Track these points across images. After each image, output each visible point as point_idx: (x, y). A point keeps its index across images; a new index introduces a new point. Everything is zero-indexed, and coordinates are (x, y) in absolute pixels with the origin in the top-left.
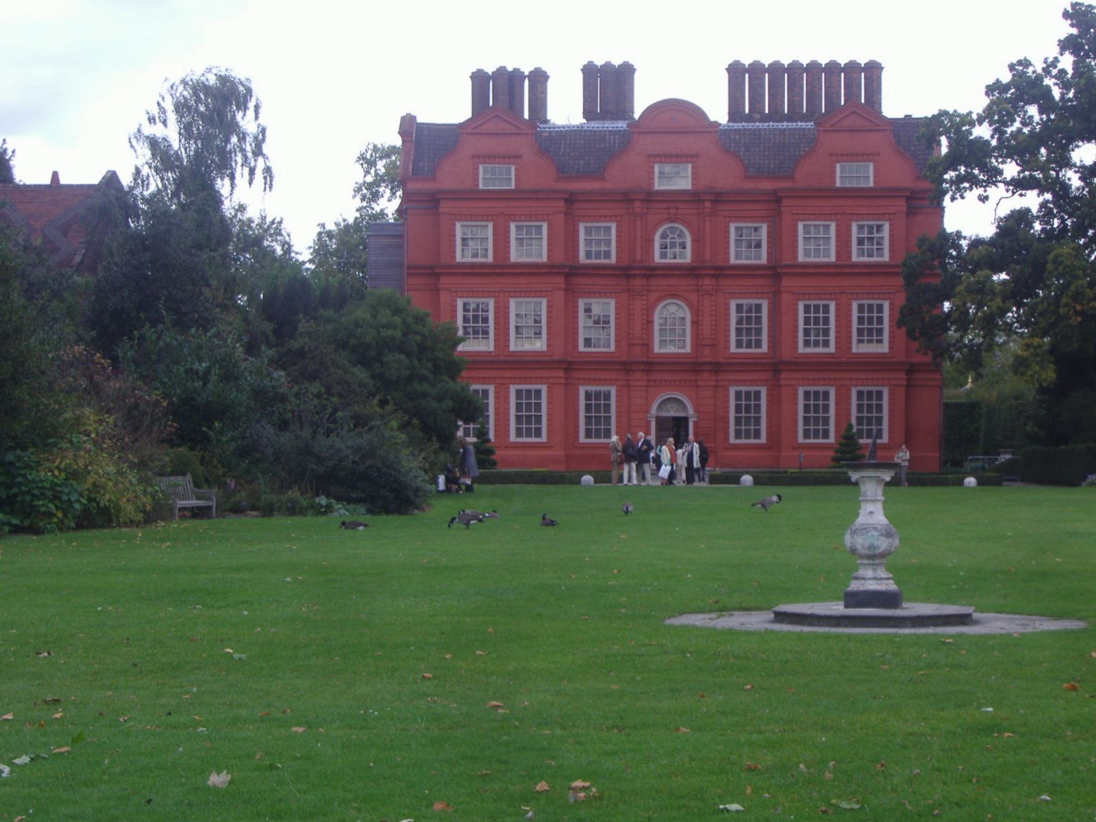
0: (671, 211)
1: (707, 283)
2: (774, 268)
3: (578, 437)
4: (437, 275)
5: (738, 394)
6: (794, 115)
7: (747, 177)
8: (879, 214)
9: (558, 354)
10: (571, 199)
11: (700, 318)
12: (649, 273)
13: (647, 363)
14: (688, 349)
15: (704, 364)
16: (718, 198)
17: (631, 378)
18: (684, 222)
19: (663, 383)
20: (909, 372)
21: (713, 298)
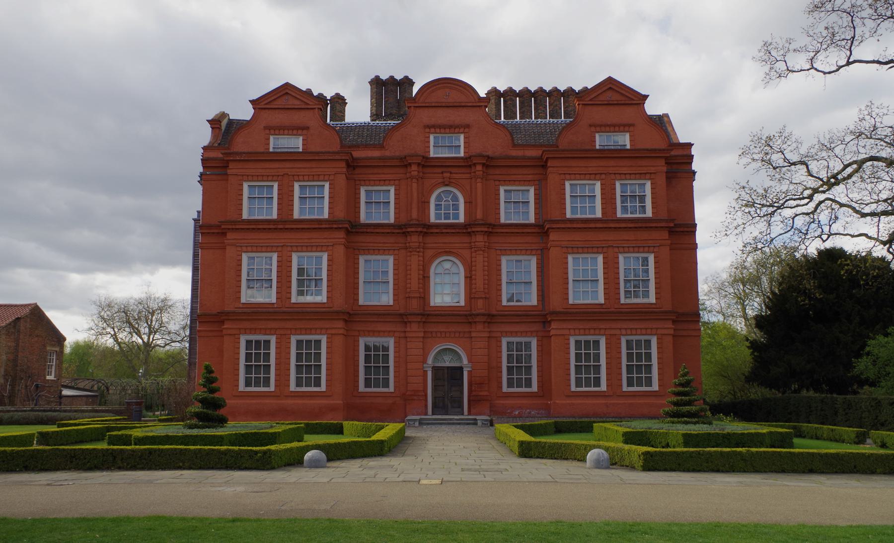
2: (541, 227)
3: (358, 386)
4: (224, 234)
7: (515, 146)
8: (641, 174)
11: (473, 272)
12: (425, 230)
13: (423, 315)
15: (478, 315)
17: (408, 329)
18: (457, 186)
19: (439, 335)
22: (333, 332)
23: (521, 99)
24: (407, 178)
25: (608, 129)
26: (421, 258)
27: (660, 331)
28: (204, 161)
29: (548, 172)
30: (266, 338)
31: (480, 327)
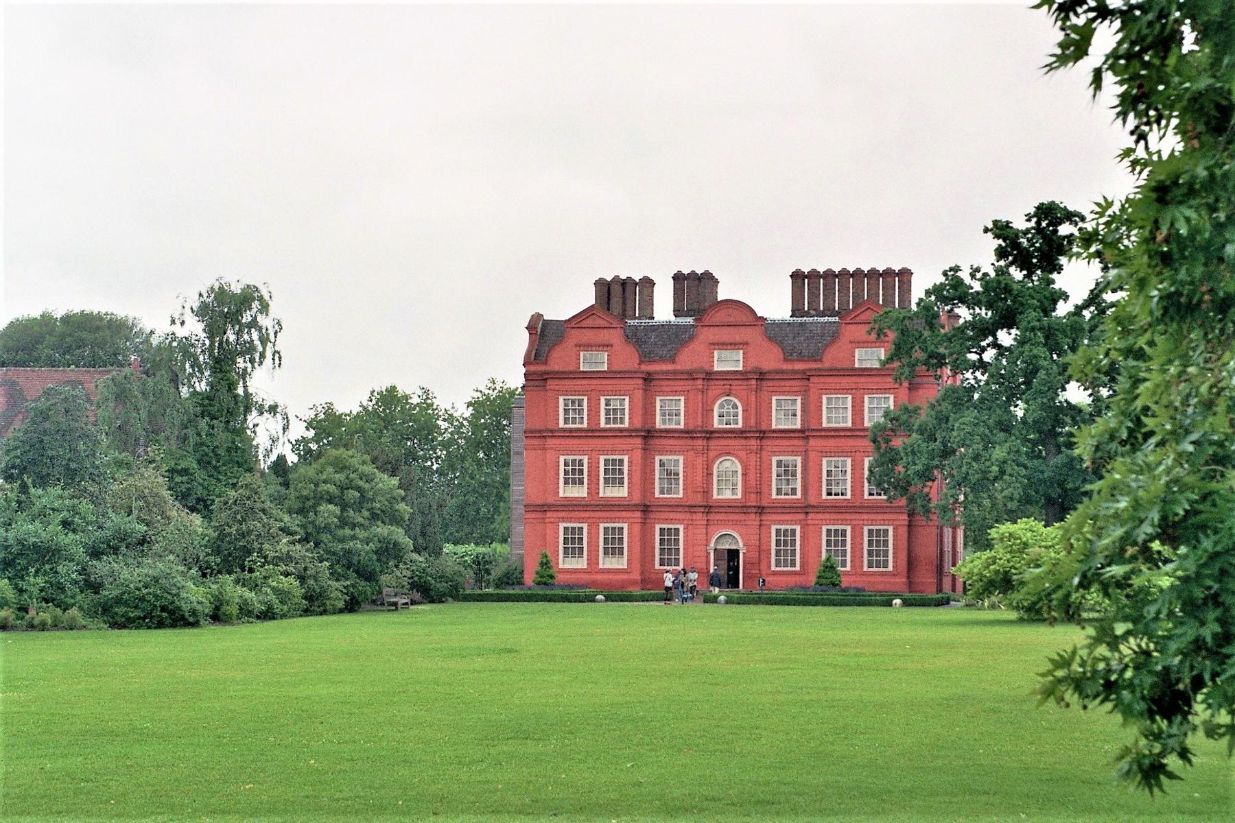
5: (778, 531)
6: (829, 311)
7: (785, 360)
9: (637, 499)
10: (648, 379)
14: (739, 496)
15: (750, 507)
16: (762, 376)
18: (736, 396)
21: (758, 456)
22: (633, 520)
27: (895, 522)
30: (580, 525)
31: (753, 516)
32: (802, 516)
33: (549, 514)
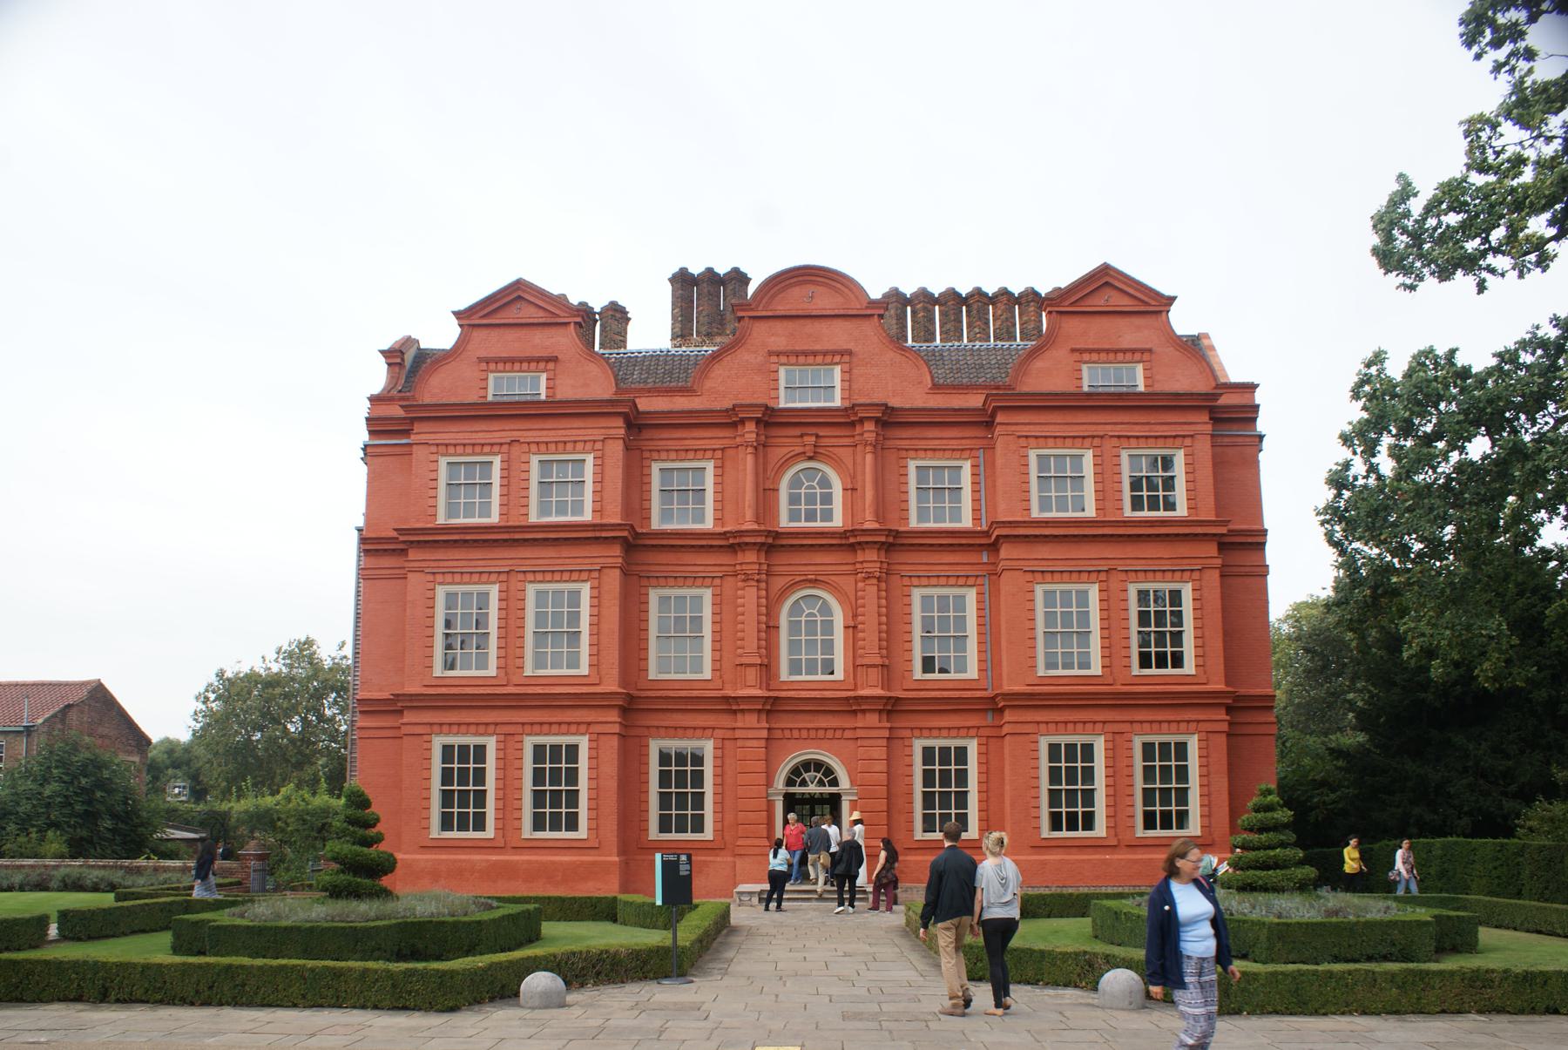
0: (806, 438)
1: (870, 559)
2: (986, 534)
7: (936, 387)
12: (770, 541)
16: (889, 419)
20: (1229, 709)
21: (883, 585)
23: (943, 308)
24: (737, 447)
25: (1103, 356)
26: (763, 593)
28: (369, 420)
29: (996, 433)
30: (479, 740)
32: (973, 720)
33: (409, 717)
